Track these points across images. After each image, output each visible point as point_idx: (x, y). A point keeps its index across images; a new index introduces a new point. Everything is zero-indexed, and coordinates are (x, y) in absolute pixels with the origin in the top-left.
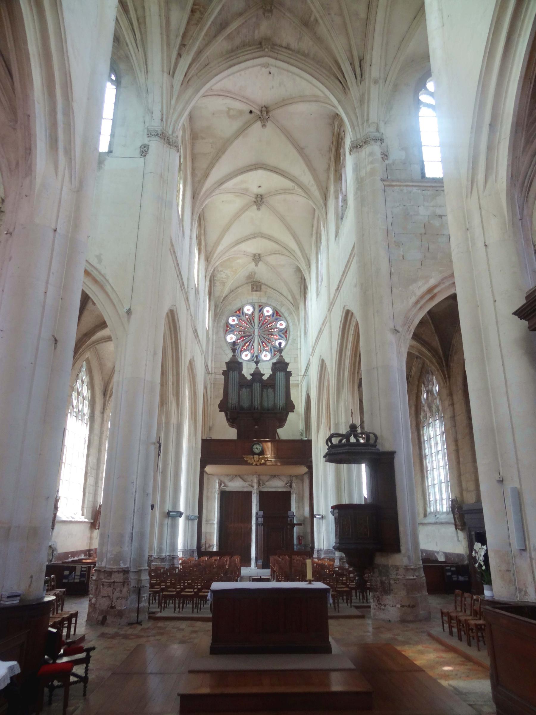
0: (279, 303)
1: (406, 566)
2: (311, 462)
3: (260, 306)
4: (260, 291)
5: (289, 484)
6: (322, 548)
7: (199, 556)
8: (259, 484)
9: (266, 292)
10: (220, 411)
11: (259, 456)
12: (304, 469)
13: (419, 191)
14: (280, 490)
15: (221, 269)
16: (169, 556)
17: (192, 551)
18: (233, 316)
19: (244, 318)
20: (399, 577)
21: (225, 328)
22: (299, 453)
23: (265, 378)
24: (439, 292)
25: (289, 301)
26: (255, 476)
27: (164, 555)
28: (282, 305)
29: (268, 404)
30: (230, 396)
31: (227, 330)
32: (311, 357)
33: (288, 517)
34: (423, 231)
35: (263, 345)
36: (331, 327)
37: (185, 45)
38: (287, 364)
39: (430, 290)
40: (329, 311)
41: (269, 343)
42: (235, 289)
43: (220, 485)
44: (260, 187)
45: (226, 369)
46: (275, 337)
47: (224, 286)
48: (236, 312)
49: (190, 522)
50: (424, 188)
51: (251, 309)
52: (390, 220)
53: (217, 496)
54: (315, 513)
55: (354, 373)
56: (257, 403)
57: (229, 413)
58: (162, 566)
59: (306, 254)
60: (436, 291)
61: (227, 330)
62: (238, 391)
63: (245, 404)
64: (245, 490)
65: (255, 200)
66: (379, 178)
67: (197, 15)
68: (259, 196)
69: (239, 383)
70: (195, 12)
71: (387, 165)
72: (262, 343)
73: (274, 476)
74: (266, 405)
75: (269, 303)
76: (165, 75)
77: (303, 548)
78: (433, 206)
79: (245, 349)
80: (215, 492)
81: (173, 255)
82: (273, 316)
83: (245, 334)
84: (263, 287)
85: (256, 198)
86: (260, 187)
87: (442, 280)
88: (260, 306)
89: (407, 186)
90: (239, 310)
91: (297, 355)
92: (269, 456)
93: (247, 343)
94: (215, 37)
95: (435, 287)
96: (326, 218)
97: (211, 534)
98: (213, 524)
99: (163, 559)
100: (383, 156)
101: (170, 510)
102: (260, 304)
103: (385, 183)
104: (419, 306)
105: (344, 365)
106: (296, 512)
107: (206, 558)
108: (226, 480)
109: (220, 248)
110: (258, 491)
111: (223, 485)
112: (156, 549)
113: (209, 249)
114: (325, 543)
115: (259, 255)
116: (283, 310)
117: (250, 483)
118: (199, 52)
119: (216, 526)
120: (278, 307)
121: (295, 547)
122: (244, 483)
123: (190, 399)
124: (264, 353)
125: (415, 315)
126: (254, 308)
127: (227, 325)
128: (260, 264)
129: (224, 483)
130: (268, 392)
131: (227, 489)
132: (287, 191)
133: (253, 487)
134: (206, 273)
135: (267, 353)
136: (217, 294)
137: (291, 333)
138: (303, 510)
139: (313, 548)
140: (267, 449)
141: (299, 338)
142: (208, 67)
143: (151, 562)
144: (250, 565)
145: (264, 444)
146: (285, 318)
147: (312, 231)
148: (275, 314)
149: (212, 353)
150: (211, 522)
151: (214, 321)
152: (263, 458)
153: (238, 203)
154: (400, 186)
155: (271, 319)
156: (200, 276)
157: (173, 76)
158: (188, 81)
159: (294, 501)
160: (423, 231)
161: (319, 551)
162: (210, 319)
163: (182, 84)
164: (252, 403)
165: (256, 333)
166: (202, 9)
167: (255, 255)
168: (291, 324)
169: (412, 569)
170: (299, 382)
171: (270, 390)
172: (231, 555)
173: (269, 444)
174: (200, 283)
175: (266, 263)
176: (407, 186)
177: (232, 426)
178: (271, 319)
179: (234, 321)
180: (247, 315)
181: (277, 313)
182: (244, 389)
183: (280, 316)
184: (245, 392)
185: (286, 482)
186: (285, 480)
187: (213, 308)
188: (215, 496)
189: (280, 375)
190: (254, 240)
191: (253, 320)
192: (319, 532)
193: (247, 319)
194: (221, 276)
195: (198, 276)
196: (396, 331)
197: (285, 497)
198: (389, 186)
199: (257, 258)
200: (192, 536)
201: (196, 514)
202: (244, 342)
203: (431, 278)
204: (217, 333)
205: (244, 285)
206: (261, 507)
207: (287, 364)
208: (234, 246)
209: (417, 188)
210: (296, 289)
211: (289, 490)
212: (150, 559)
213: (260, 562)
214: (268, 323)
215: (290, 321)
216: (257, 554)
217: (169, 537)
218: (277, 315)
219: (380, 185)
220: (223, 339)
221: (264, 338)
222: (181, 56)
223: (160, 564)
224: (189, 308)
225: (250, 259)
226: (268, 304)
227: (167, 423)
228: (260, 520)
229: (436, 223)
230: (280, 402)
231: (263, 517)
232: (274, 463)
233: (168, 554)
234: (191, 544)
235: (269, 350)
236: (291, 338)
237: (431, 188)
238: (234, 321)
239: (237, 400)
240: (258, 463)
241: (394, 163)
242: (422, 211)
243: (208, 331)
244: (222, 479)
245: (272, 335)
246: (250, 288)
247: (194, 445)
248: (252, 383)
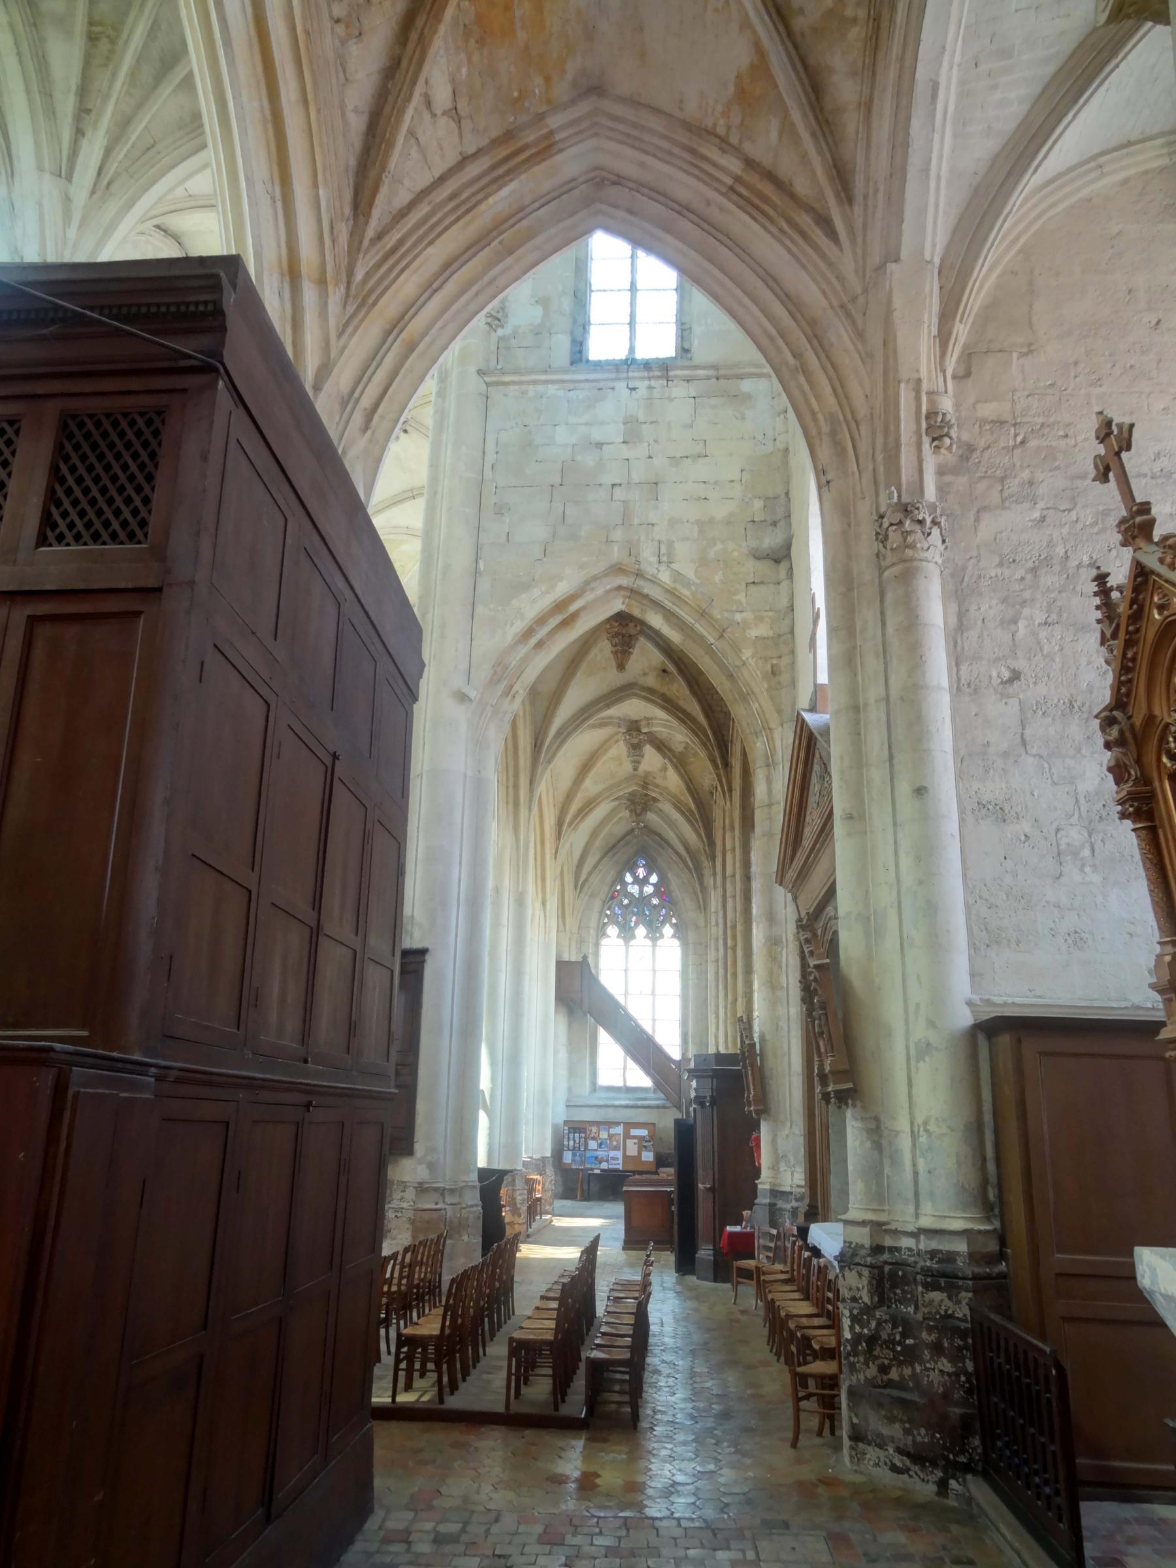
1: (421, 1183)
13: (561, 393)
20: (405, 1205)
24: (583, 608)
34: (557, 479)
37: (88, 111)
39: (560, 606)
50: (571, 386)
52: (490, 457)
60: (573, 608)
66: (472, 369)
67: (104, 45)
70: (97, 39)
71: (500, 339)
76: (47, 177)
78: (586, 424)
87: (587, 583)
89: (535, 382)
94: (155, 87)
95: (572, 598)
100: (490, 320)
103: (487, 379)
104: (533, 641)
118: (124, 124)
125: (525, 660)
142: (151, 153)
154: (520, 383)
157: (69, 178)
158: (109, 184)
160: (557, 479)
163: (93, 192)
166: (110, 32)
169: (436, 1189)
176: (535, 382)
196: (462, 697)
198: (498, 384)
203: (561, 580)
209: (556, 386)
219: (475, 384)
222: (83, 135)
229: (589, 460)
237: (587, 385)
241: (515, 334)
242: (562, 436)
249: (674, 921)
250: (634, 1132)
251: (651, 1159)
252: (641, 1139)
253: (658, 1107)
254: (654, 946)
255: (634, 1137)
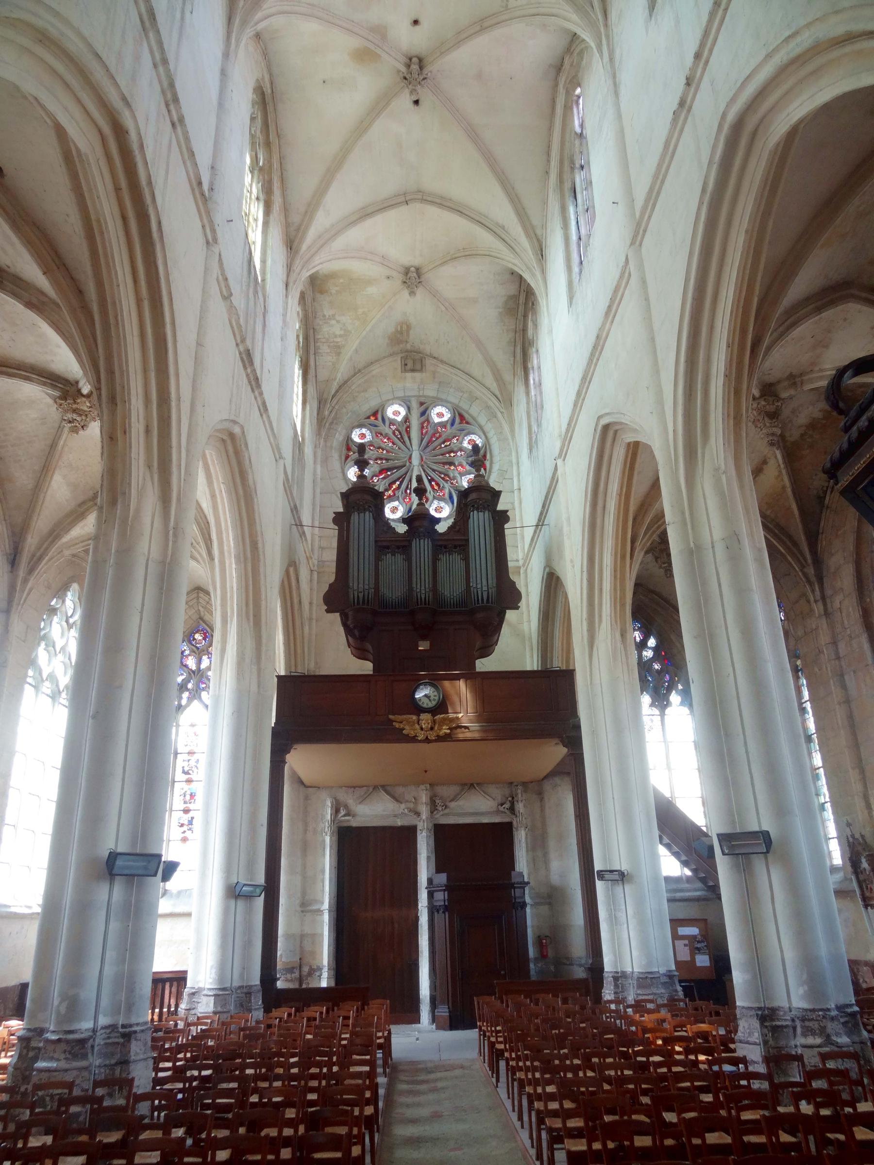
0: (465, 395)
2: (578, 727)
3: (422, 404)
4: (421, 370)
5: (507, 805)
6: (629, 969)
7: (267, 1010)
8: (433, 806)
9: (434, 373)
10: (328, 611)
11: (434, 715)
12: (557, 752)
14: (485, 820)
15: (331, 312)
16: (112, 1027)
17: (247, 992)
18: (361, 426)
19: (386, 430)
21: (344, 452)
22: (542, 706)
23: (441, 528)
25: (489, 389)
26: (423, 787)
27: (87, 1025)
28: (473, 399)
29: (451, 588)
30: (353, 570)
31: (347, 457)
32: (560, 462)
33: (512, 886)
35: (432, 486)
36: (644, 282)
38: (496, 495)
40: (632, 243)
41: (446, 481)
42: (365, 367)
43: (337, 811)
44: (416, 22)
45: (341, 510)
46: (460, 468)
47: (338, 354)
48: (369, 418)
49: (241, 904)
51: (403, 412)
53: (328, 841)
54: (598, 866)
55: (737, 392)
56: (422, 588)
57: (350, 613)
58: (69, 1077)
59: (533, 227)
61: (347, 457)
62: (372, 559)
63: (393, 591)
64: (399, 823)
65: (403, 69)
68: (415, 60)
69: (376, 542)
72: (430, 481)
73: (470, 786)
74: (447, 593)
75: (443, 397)
77: (552, 968)
79: (390, 496)
80: (323, 830)
81: (189, 164)
82: (452, 424)
83: (390, 464)
84: (428, 362)
85: (408, 66)
86: (416, 22)
88: (422, 404)
90: (375, 414)
91: (513, 503)
92: (460, 715)
93: (394, 482)
96: (606, 25)
97: (315, 938)
98: (320, 912)
99: (82, 1042)
101: (120, 850)
102: (422, 399)
105: (708, 360)
106: (529, 875)
107: (283, 1013)
108: (350, 800)
109: (321, 222)
110: (431, 825)
111: (342, 812)
112: (56, 1003)
113: (295, 218)
114: (635, 953)
115: (418, 270)
116: (474, 411)
117: (411, 806)
119: (326, 917)
120: (464, 405)
121: (532, 966)
122: (396, 805)
123: (241, 559)
124: (436, 503)
126: (409, 409)
127: (348, 444)
128: (420, 292)
129: (346, 807)
130: (451, 562)
131: (355, 823)
132: (486, 24)
133: (418, 814)
134: (288, 276)
135: (442, 504)
136: (323, 374)
137: (496, 459)
138: (547, 869)
139: (596, 969)
140: (456, 699)
141: (515, 468)
143: (36, 1059)
144: (417, 1020)
145: (447, 684)
146: (481, 428)
147: (549, 161)
148: (458, 420)
149: (314, 504)
150: (315, 907)
151: (318, 433)
152: (443, 722)
153: (365, 85)
155: (449, 430)
156: (269, 262)
159: (524, 845)
161: (619, 978)
162: (307, 422)
164: (411, 589)
165: (415, 461)
167: (407, 271)
168: (494, 441)
170: (521, 563)
171: (456, 559)
172: (363, 997)
173: (462, 684)
174: (268, 276)
175: (434, 294)
177: (360, 653)
178: (449, 430)
179: (363, 436)
180: (392, 422)
181: (462, 417)
182: (389, 556)
183: (467, 423)
184: (393, 563)
185: (499, 799)
186: (498, 793)
187: (313, 404)
188: (324, 841)
189: (479, 520)
190: (404, 209)
191: (408, 433)
192: (614, 920)
193: (394, 433)
194: (330, 330)
195: (263, 261)
197: (500, 836)
199: (413, 278)
200: (248, 945)
201: (261, 879)
202: (387, 482)
204: (326, 460)
205: (385, 357)
206: (441, 863)
207: (496, 495)
208: (353, 223)
210: (502, 359)
211: (506, 820)
212: (34, 1044)
213: (443, 1011)
214: (441, 440)
215: (491, 434)
216: (433, 987)
217: (110, 954)
218: (460, 418)
220: (340, 475)
221: (434, 470)
223: (63, 1064)
224: (215, 240)
225: (399, 278)
226: (442, 400)
227: (125, 552)
228: (440, 896)
230: (483, 582)
231: (448, 888)
232: (476, 735)
233: (103, 1021)
234: (245, 969)
235: (447, 496)
236: (496, 467)
238: (363, 436)
239: (372, 581)
240: (432, 737)
243: (298, 446)
244: (342, 796)
245: (451, 464)
246: (398, 363)
247: (254, 688)
248: (410, 542)
249: (680, 687)
250: (683, 931)
251: (708, 964)
252: (692, 938)
253: (698, 899)
254: (662, 715)
255: (683, 937)
